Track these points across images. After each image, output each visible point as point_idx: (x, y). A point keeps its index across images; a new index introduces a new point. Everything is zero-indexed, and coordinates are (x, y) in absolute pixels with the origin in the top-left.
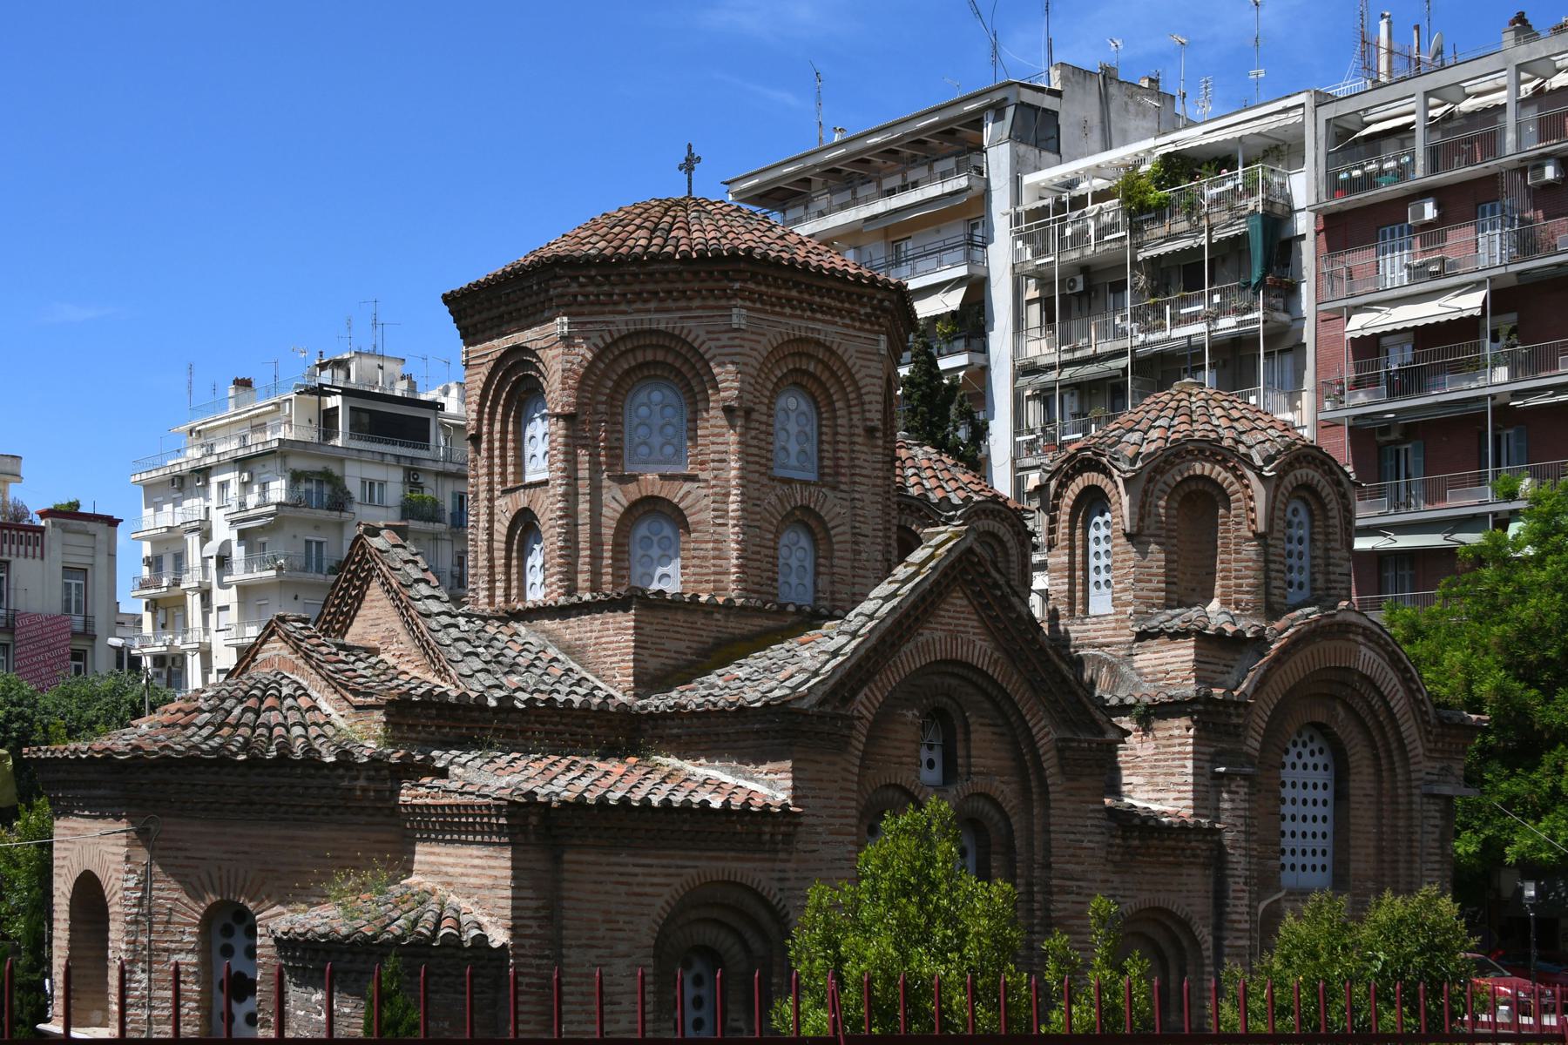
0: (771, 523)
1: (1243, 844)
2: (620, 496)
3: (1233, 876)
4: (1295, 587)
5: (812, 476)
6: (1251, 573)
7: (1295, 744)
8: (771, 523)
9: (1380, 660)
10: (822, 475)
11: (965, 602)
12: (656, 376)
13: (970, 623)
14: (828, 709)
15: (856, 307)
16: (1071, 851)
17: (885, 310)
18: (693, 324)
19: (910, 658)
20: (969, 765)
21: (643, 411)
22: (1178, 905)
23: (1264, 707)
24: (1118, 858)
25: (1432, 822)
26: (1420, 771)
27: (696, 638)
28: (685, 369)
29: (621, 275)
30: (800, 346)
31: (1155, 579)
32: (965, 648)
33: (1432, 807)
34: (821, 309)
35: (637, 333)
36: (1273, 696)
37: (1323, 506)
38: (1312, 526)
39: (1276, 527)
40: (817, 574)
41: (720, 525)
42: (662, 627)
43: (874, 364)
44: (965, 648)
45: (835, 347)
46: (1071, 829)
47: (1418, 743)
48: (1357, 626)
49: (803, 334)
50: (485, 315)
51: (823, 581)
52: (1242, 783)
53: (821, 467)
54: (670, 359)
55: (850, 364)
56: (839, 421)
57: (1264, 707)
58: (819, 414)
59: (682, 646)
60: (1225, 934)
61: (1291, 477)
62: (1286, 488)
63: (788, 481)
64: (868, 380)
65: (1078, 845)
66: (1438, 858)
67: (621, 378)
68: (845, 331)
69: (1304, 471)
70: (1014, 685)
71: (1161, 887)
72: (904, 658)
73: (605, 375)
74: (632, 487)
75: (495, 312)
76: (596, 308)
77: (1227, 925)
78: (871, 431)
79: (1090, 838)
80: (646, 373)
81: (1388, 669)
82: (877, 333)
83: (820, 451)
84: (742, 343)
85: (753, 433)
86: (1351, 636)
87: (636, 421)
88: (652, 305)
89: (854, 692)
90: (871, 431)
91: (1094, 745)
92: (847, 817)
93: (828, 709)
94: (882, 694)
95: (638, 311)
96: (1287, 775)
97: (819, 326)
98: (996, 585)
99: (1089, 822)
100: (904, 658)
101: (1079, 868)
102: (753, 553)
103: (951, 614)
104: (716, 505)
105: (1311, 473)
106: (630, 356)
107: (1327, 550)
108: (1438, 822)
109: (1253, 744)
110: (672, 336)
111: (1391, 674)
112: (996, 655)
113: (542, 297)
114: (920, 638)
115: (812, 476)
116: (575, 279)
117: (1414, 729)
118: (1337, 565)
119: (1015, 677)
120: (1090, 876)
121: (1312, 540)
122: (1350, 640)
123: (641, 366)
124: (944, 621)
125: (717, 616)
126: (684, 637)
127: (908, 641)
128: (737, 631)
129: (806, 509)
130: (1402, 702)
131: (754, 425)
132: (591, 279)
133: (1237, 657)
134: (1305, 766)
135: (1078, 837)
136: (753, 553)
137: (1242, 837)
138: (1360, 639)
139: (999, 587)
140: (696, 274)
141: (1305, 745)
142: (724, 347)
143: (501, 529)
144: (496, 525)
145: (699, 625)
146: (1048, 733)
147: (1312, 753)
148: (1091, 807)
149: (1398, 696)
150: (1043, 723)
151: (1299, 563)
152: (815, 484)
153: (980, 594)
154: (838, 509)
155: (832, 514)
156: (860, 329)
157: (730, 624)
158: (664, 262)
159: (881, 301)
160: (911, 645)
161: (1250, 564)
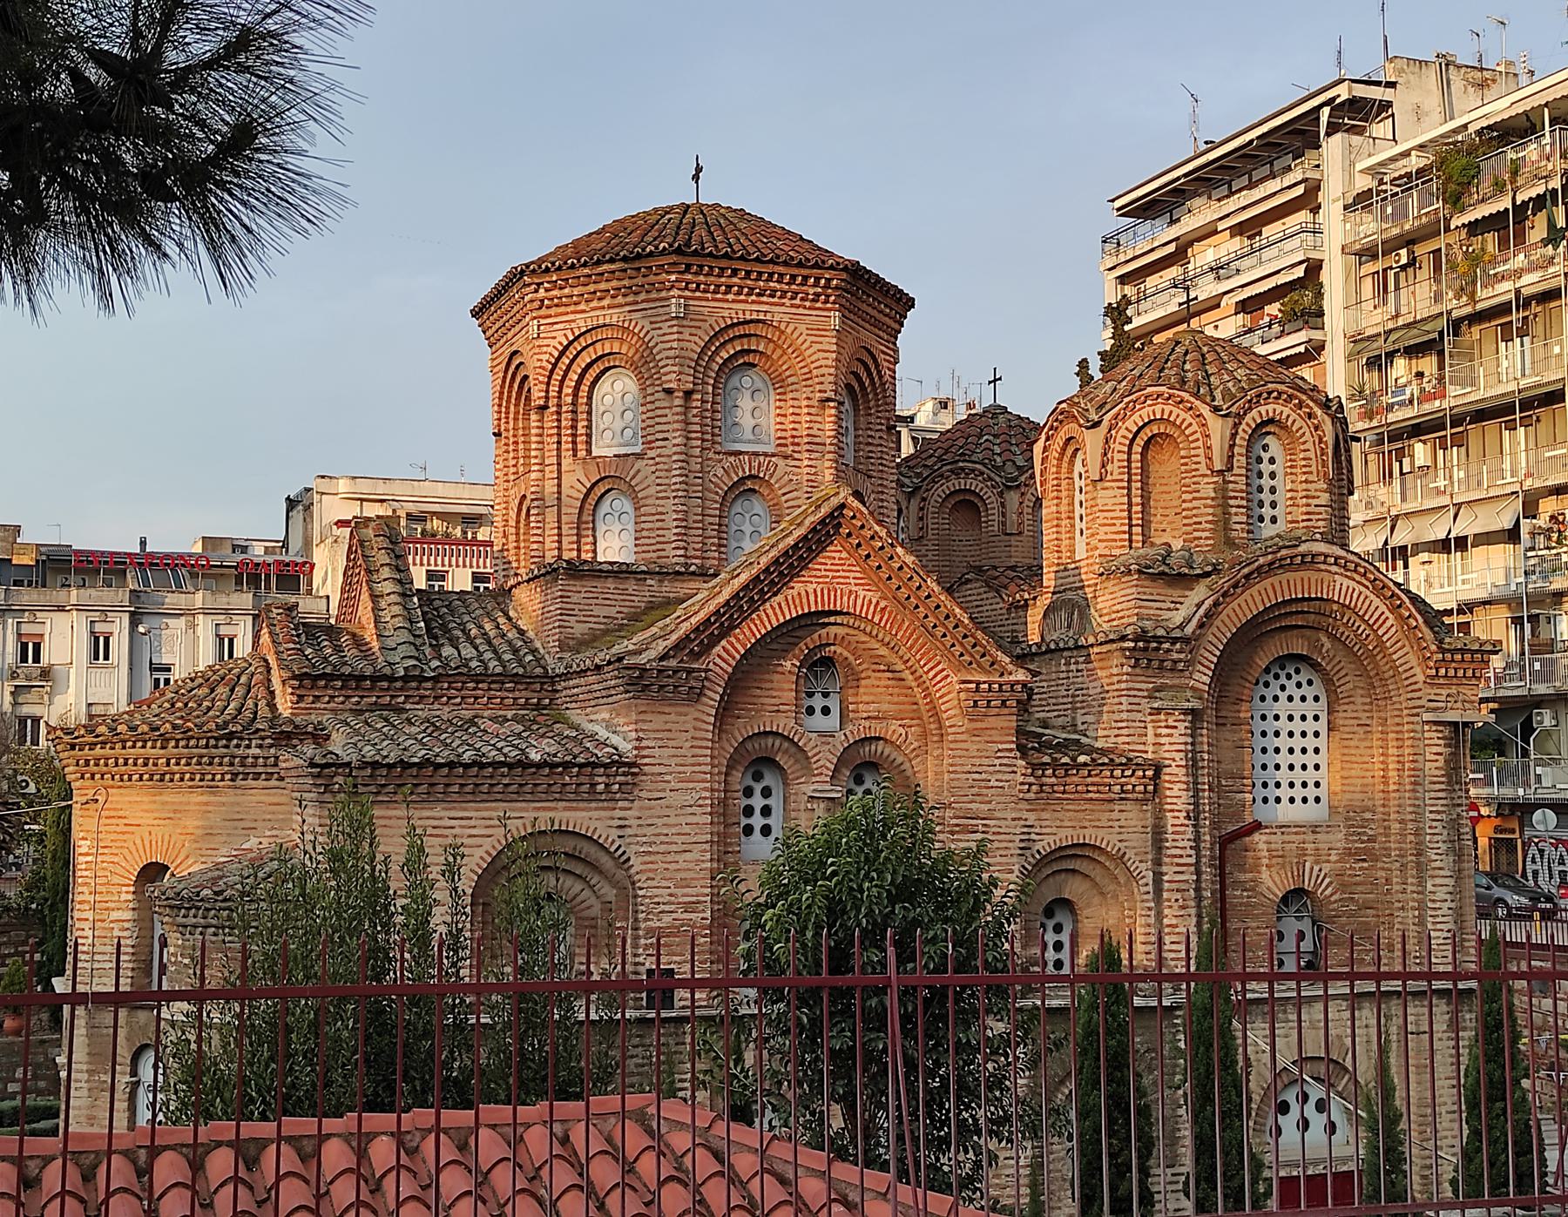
0: (717, 493)
1: (1184, 779)
2: (584, 480)
3: (1172, 811)
6: (1211, 511)
7: (1277, 677)
8: (717, 493)
9: (1362, 589)
14: (673, 663)
22: (1108, 839)
23: (1215, 641)
24: (1032, 795)
25: (1435, 749)
26: (1420, 698)
27: (627, 603)
31: (1118, 522)
32: (845, 598)
33: (1435, 735)
36: (1224, 629)
39: (1235, 464)
41: (662, 498)
42: (591, 595)
43: (827, 339)
44: (845, 598)
45: (783, 326)
46: (974, 769)
47: (1417, 670)
49: (748, 317)
52: (1182, 717)
57: (1215, 641)
59: (612, 612)
60: (1164, 869)
62: (1248, 424)
63: (738, 453)
65: (983, 784)
66: (1443, 787)
69: (1270, 407)
71: (1087, 824)
72: (770, 611)
76: (562, 309)
77: (1167, 860)
79: (999, 776)
81: (1372, 597)
84: (681, 330)
85: (695, 411)
86: (1323, 567)
89: (706, 648)
92: (700, 765)
93: (673, 663)
94: (744, 646)
97: (765, 308)
99: (997, 762)
100: (770, 611)
101: (986, 807)
102: (694, 522)
103: (828, 567)
104: (658, 481)
108: (1439, 750)
109: (1202, 678)
112: (883, 604)
117: (1411, 656)
120: (998, 814)
124: (818, 573)
125: (649, 582)
126: (613, 603)
127: (775, 594)
128: (671, 595)
130: (1394, 629)
133: (1187, 593)
134: (1290, 699)
136: (694, 522)
137: (1184, 771)
138: (1334, 569)
141: (1289, 677)
142: (664, 335)
145: (630, 591)
147: (1299, 685)
148: (1000, 746)
149: (1388, 624)
150: (940, 667)
151: (1272, 497)
156: (810, 308)
157: (664, 589)
159: (829, 281)
161: (1209, 502)
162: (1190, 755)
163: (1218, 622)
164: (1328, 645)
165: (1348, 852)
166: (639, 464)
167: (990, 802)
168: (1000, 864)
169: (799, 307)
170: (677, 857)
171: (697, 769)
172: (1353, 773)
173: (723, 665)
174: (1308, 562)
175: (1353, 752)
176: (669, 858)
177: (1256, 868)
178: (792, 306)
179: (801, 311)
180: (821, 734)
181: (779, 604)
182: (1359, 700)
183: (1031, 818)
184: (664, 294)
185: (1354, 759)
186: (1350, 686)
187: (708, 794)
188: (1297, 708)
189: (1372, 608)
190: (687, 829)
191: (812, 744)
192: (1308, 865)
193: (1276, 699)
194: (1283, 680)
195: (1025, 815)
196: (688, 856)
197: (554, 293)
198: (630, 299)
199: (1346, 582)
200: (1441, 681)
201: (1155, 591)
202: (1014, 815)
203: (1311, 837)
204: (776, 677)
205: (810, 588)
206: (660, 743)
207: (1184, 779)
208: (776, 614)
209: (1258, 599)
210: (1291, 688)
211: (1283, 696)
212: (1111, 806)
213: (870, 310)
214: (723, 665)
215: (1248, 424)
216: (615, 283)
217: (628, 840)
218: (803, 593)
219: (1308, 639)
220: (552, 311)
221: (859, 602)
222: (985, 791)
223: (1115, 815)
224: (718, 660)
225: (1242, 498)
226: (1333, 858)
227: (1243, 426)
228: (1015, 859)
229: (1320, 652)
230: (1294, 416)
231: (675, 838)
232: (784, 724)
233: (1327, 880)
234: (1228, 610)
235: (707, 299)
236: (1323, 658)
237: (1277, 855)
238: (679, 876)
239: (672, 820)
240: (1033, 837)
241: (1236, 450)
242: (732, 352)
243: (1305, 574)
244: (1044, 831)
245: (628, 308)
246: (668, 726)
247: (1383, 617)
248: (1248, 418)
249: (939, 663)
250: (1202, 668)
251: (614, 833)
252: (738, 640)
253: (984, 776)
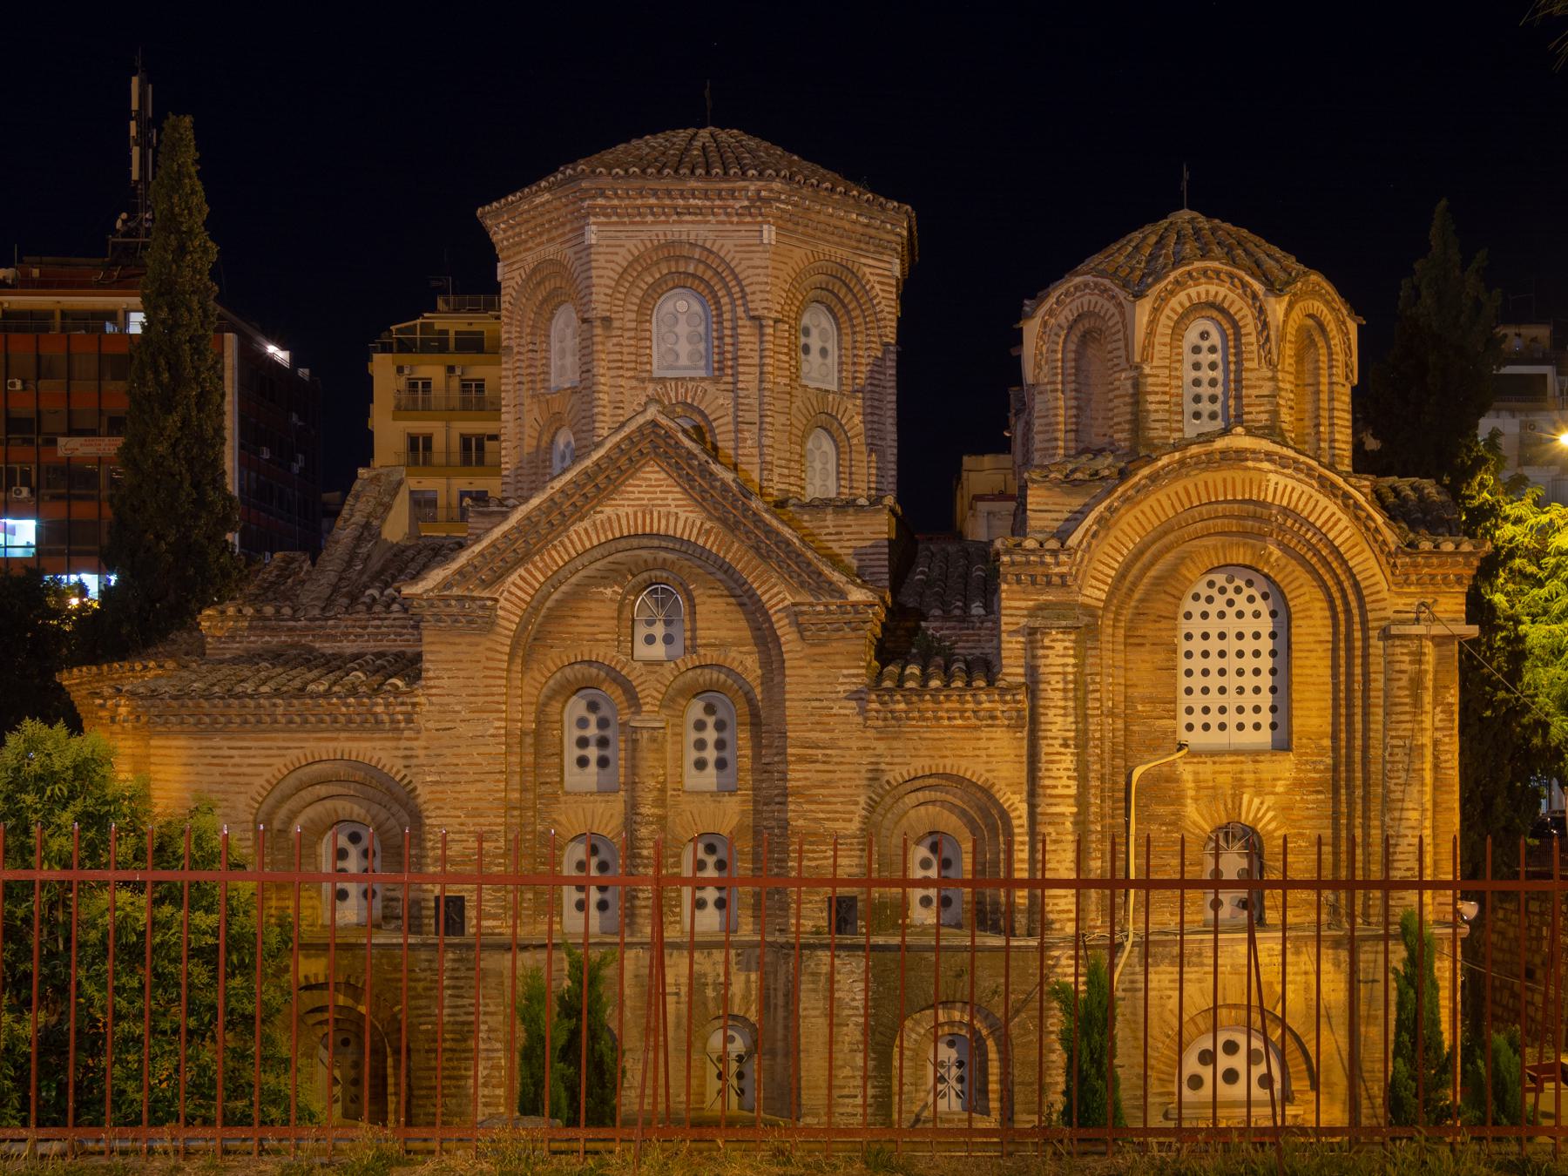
1: (1061, 703)
4: (1205, 417)
7: (1222, 591)
9: (1306, 488)
11: (663, 475)
13: (670, 496)
15: (731, 202)
16: (813, 719)
17: (767, 201)
19: (581, 535)
30: (671, 251)
32: (663, 522)
34: (689, 211)
36: (1125, 540)
44: (663, 522)
48: (1253, 452)
52: (1060, 636)
55: (728, 259)
56: (854, 314)
57: (1112, 552)
61: (1182, 296)
62: (1173, 310)
64: (750, 272)
68: (720, 227)
69: (1202, 289)
70: (735, 553)
71: (948, 753)
72: (575, 537)
81: (1317, 496)
82: (761, 223)
86: (1250, 464)
91: (833, 608)
96: (1185, 626)
100: (575, 537)
105: (1213, 289)
111: (1324, 501)
112: (708, 525)
114: (599, 516)
118: (1255, 387)
119: (736, 545)
120: (841, 744)
122: (1247, 468)
127: (581, 519)
131: (615, 332)
135: (825, 703)
138: (1266, 465)
139: (695, 457)
141: (1238, 590)
146: (783, 600)
147: (1251, 599)
148: (845, 672)
149: (1341, 526)
150: (775, 590)
151: (1211, 391)
152: (702, 379)
154: (721, 401)
155: (713, 407)
160: (586, 523)
162: (1071, 677)
163: (1115, 532)
164: (1277, 553)
165: (1298, 784)
167: (833, 731)
168: (844, 795)
169: (723, 223)
170: (468, 787)
171: (490, 699)
172: (1307, 695)
173: (519, 593)
174: (1237, 457)
175: (1308, 671)
176: (459, 788)
177: (1179, 799)
178: (719, 222)
179: (728, 227)
180: (648, 663)
181: (586, 530)
182: (1318, 614)
183: (881, 747)
185: (1310, 680)
186: (1307, 598)
187: (503, 724)
188: (1249, 624)
189: (1319, 510)
190: (479, 759)
191: (636, 673)
192: (1246, 798)
193: (1222, 615)
194: (1230, 594)
195: (875, 744)
196: (479, 786)
199: (1283, 481)
200: (1413, 589)
201: (1050, 501)
202: (861, 744)
203: (1250, 766)
204: (593, 605)
205: (622, 511)
206: (450, 674)
207: (1061, 703)
208: (580, 540)
209: (1166, 504)
210: (1241, 602)
211: (1231, 612)
212: (976, 734)
213: (833, 221)
214: (519, 593)
215: (1173, 310)
217: (415, 770)
218: (614, 517)
219: (1253, 547)
221: (681, 524)
222: (826, 719)
223: (982, 744)
224: (513, 589)
225: (1164, 393)
226: (1280, 789)
227: (1167, 311)
228: (861, 790)
229: (1267, 562)
230: (1231, 296)
231: (466, 768)
232: (605, 653)
233: (1271, 814)
234: (1129, 518)
235: (624, 224)
236: (1272, 568)
237: (1211, 793)
238: (470, 805)
239: (463, 750)
240: (883, 766)
241: (1158, 339)
242: (657, 276)
243: (1228, 474)
244: (896, 760)
246: (459, 657)
247: (1334, 519)
248: (1174, 302)
249: (775, 585)
250: (1094, 582)
251: (402, 762)
252: (537, 567)
253: (825, 703)
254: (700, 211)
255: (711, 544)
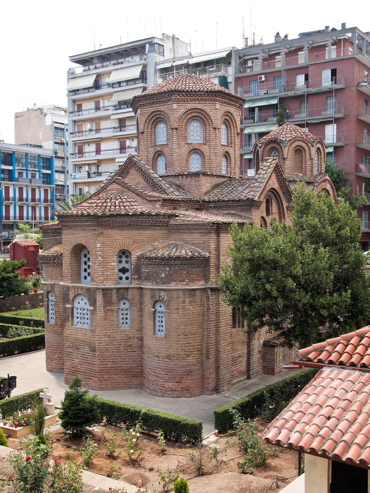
5: (226, 144)
10: (228, 144)
12: (196, 119)
18: (207, 107)
20: (272, 212)
21: (192, 128)
28: (204, 118)
29: (190, 95)
35: (191, 109)
37: (321, 153)
38: (318, 157)
40: (227, 167)
50: (148, 102)
51: (229, 169)
53: (228, 142)
54: (200, 116)
58: (228, 129)
63: (224, 146)
67: (188, 119)
73: (184, 119)
74: (191, 146)
75: (151, 101)
78: (238, 134)
80: (194, 118)
83: (228, 138)
87: (190, 130)
88: (197, 102)
90: (238, 134)
95: (193, 103)
97: (230, 108)
98: (280, 171)
106: (191, 114)
107: (321, 162)
110: (201, 110)
113: (169, 98)
115: (226, 144)
116: (179, 95)
121: (318, 160)
123: (193, 117)
129: (227, 152)
132: (183, 95)
140: (208, 95)
143: (151, 156)
144: (149, 155)
153: (277, 173)
158: (201, 92)
166: (204, 146)
184: (214, 102)
197: (182, 97)
198: (204, 102)
216: (201, 98)
220: (181, 102)
245: (204, 105)
254: (232, 105)
255: (278, 190)
